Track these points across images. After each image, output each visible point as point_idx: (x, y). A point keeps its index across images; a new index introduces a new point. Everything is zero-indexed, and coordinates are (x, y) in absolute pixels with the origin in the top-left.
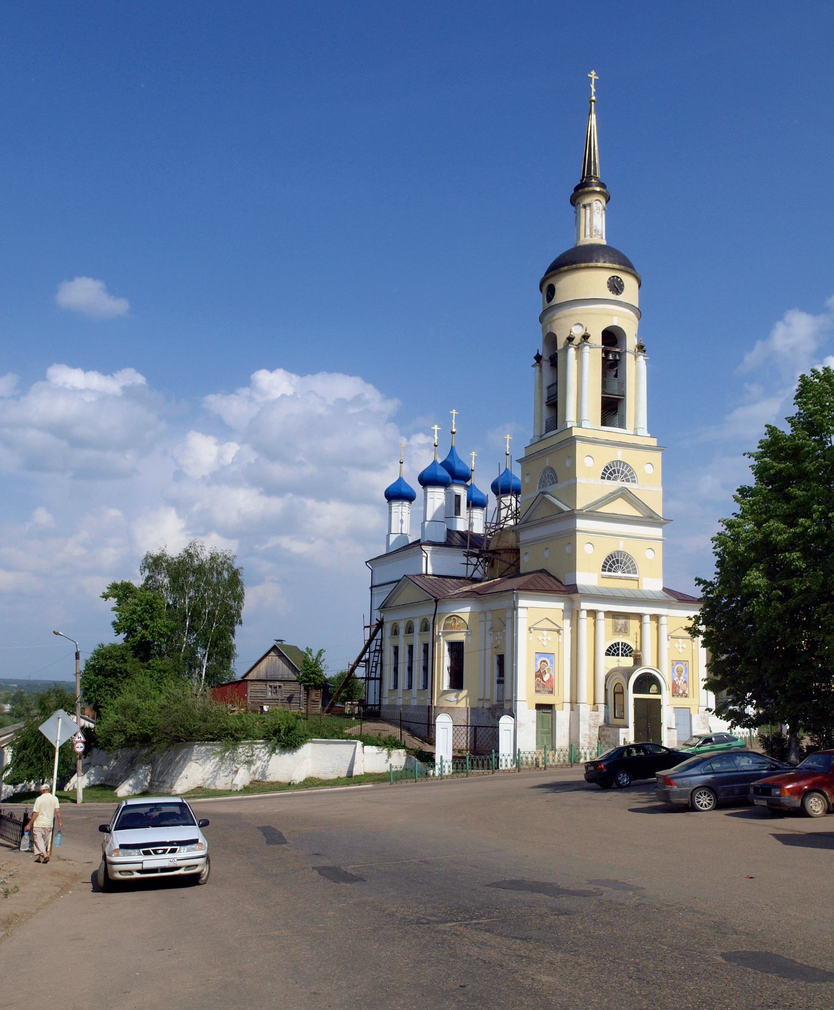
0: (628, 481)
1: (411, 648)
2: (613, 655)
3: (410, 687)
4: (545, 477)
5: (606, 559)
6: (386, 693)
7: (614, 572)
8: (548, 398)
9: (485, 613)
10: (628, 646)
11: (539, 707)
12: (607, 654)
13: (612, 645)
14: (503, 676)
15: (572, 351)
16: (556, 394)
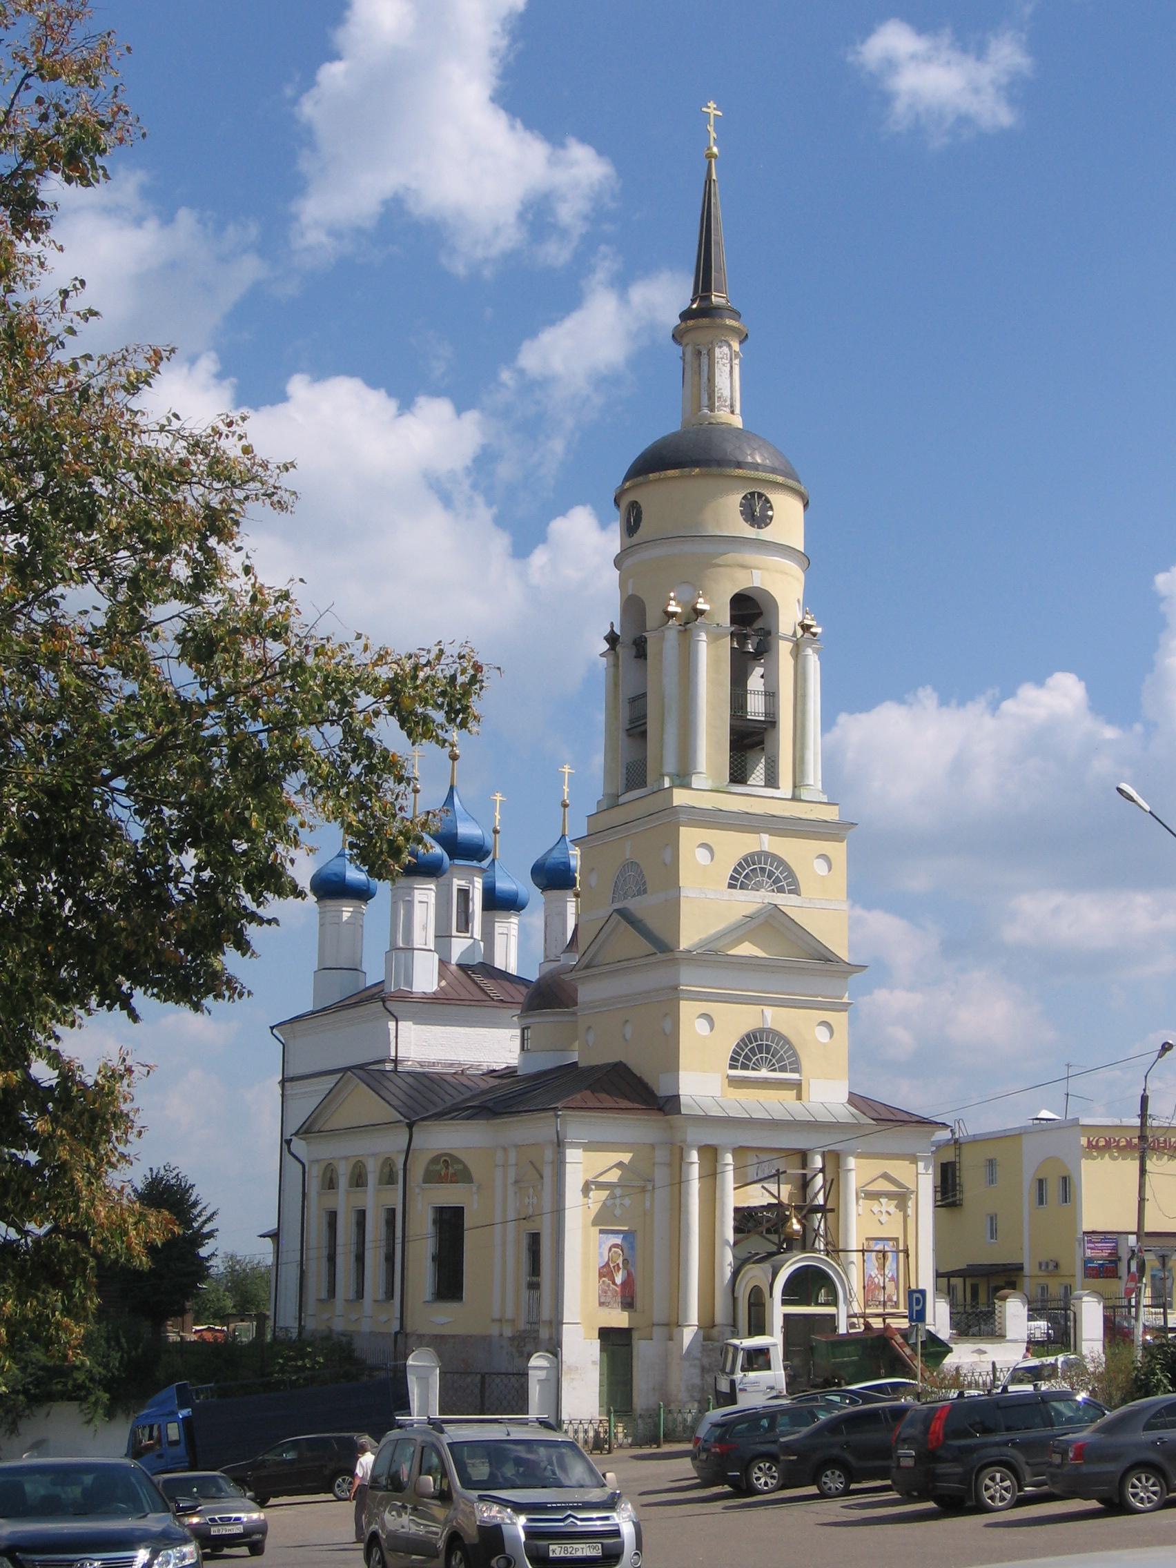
1: (362, 1214)
3: (360, 1294)
5: (738, 1045)
6: (311, 1306)
7: (753, 1069)
8: (631, 721)
9: (505, 1149)
11: (606, 1334)
14: (538, 1275)
16: (645, 716)
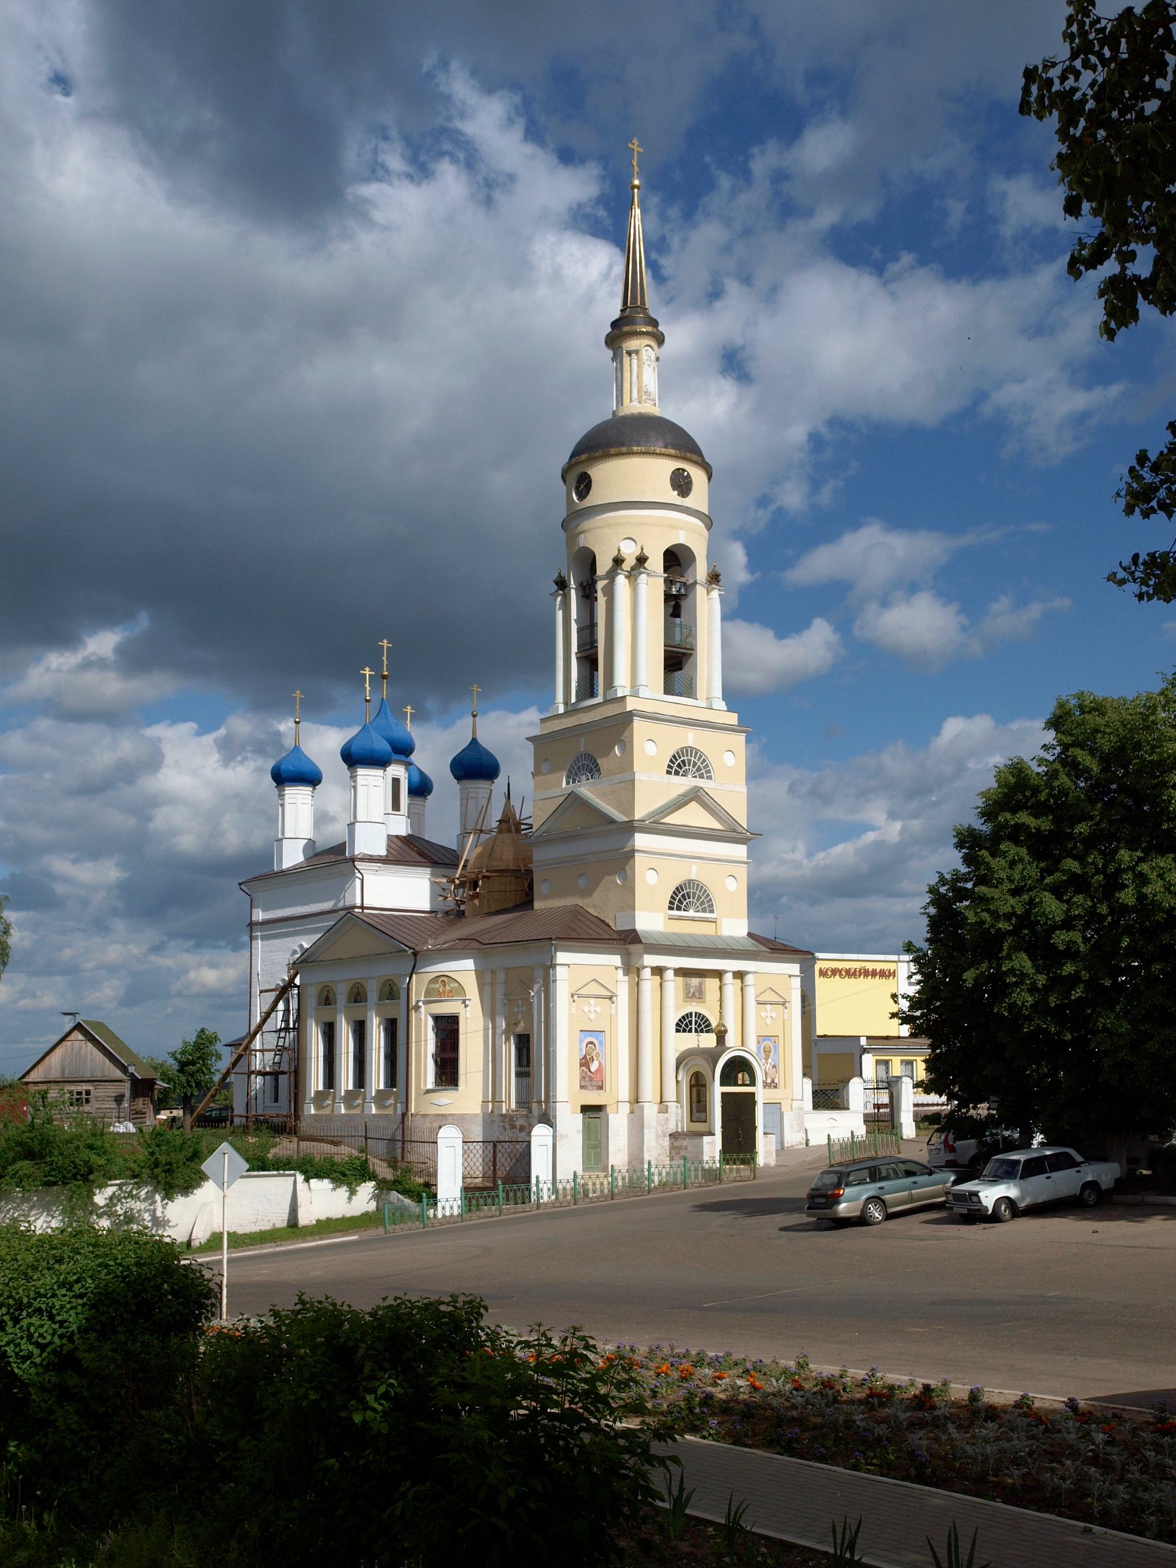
0: (701, 776)
2: (684, 1031)
4: (579, 768)
7: (684, 910)
10: (704, 1017)
12: (678, 1031)
13: (683, 1017)
15: (621, 581)
